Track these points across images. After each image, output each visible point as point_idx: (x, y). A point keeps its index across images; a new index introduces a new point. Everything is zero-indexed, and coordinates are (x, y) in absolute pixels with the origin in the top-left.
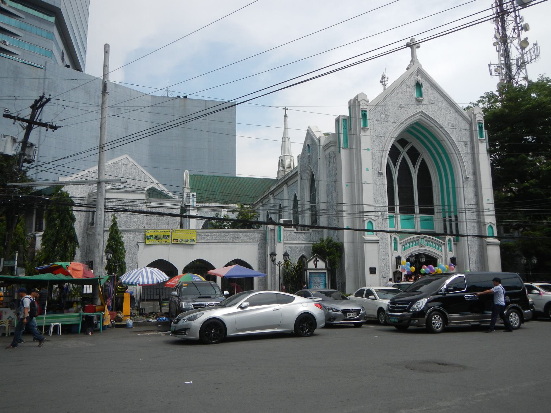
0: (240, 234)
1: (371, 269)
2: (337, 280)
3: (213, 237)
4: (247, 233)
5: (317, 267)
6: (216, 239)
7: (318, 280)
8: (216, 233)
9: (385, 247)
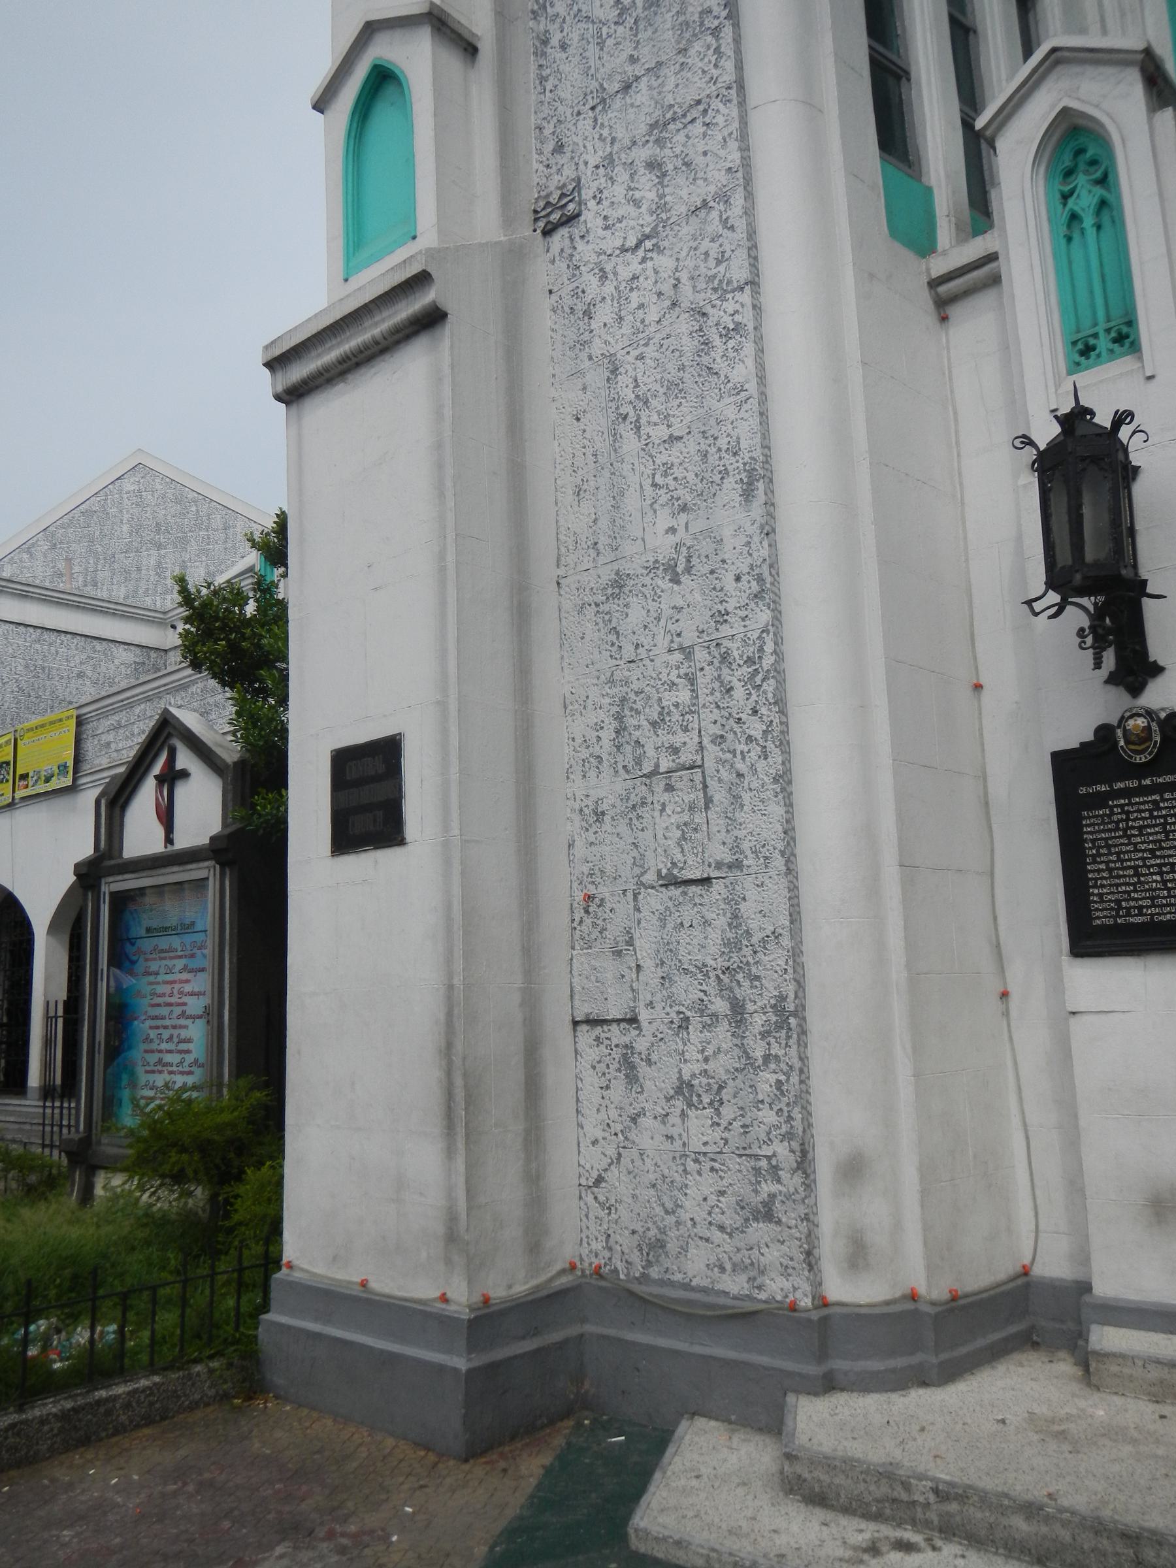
1: (343, 760)
3: (133, 735)
8: (143, 706)
9: (689, 345)
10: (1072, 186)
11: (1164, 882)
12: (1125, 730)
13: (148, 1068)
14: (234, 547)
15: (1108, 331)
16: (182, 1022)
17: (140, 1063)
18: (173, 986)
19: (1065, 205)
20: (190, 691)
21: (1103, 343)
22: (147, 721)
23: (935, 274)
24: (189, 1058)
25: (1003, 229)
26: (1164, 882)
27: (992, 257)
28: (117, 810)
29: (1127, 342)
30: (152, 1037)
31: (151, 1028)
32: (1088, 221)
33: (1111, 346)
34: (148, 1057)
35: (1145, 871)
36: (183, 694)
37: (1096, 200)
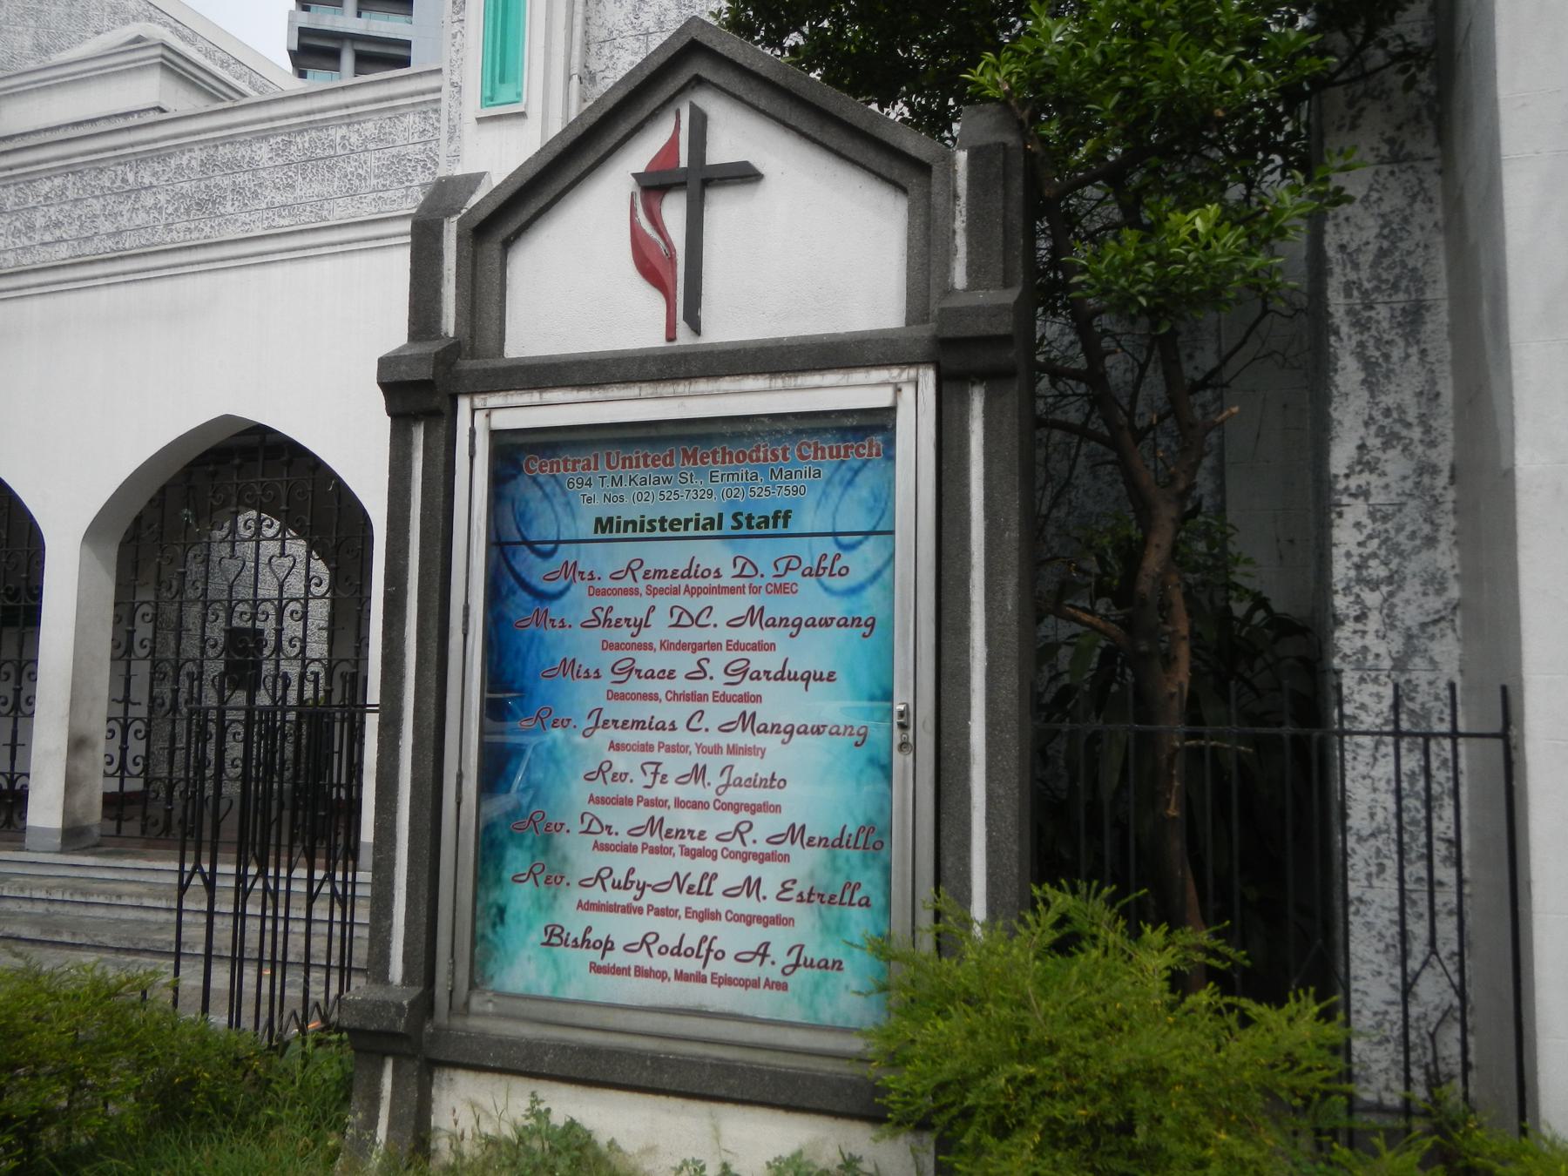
0: (262, 152)
2: (1345, 639)
3: (31, 228)
4: (323, 125)
5: (695, 327)
6: (57, 233)
7: (722, 634)
8: (58, 181)
13: (604, 838)
14: (85, 16)
16: (741, 738)
17: (576, 826)
18: (700, 654)
20: (173, 162)
22: (66, 207)
24: (765, 825)
28: (492, 248)
30: (620, 766)
31: (615, 746)
34: (607, 814)
36: (158, 168)
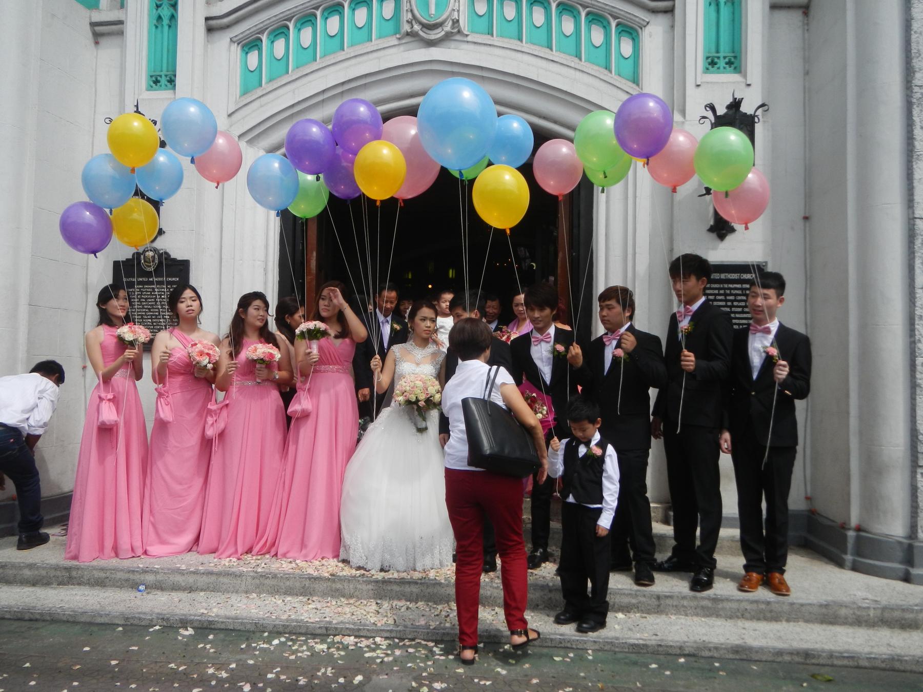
10: (161, 3)
11: (152, 322)
12: (144, 256)
15: (166, 76)
19: (157, 10)
21: (163, 81)
23: (95, 19)
25: (127, 10)
26: (152, 322)
27: (121, 22)
29: (173, 83)
32: (166, 22)
33: (166, 83)
35: (146, 317)
37: (169, 14)
